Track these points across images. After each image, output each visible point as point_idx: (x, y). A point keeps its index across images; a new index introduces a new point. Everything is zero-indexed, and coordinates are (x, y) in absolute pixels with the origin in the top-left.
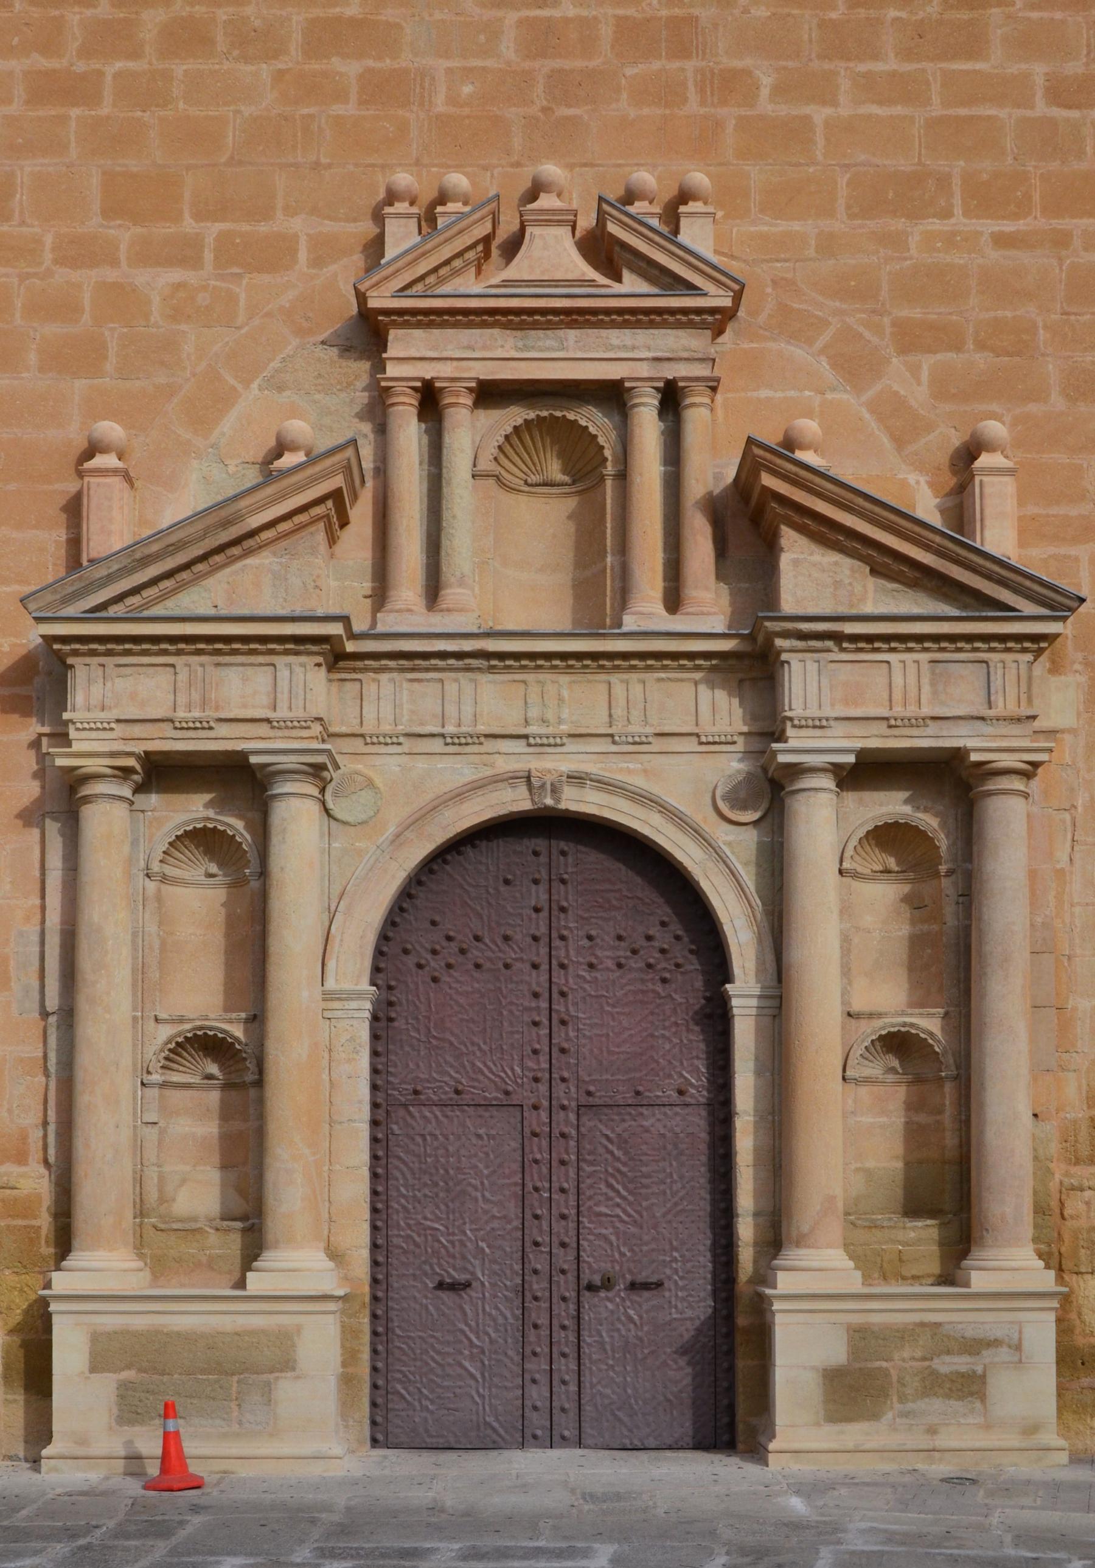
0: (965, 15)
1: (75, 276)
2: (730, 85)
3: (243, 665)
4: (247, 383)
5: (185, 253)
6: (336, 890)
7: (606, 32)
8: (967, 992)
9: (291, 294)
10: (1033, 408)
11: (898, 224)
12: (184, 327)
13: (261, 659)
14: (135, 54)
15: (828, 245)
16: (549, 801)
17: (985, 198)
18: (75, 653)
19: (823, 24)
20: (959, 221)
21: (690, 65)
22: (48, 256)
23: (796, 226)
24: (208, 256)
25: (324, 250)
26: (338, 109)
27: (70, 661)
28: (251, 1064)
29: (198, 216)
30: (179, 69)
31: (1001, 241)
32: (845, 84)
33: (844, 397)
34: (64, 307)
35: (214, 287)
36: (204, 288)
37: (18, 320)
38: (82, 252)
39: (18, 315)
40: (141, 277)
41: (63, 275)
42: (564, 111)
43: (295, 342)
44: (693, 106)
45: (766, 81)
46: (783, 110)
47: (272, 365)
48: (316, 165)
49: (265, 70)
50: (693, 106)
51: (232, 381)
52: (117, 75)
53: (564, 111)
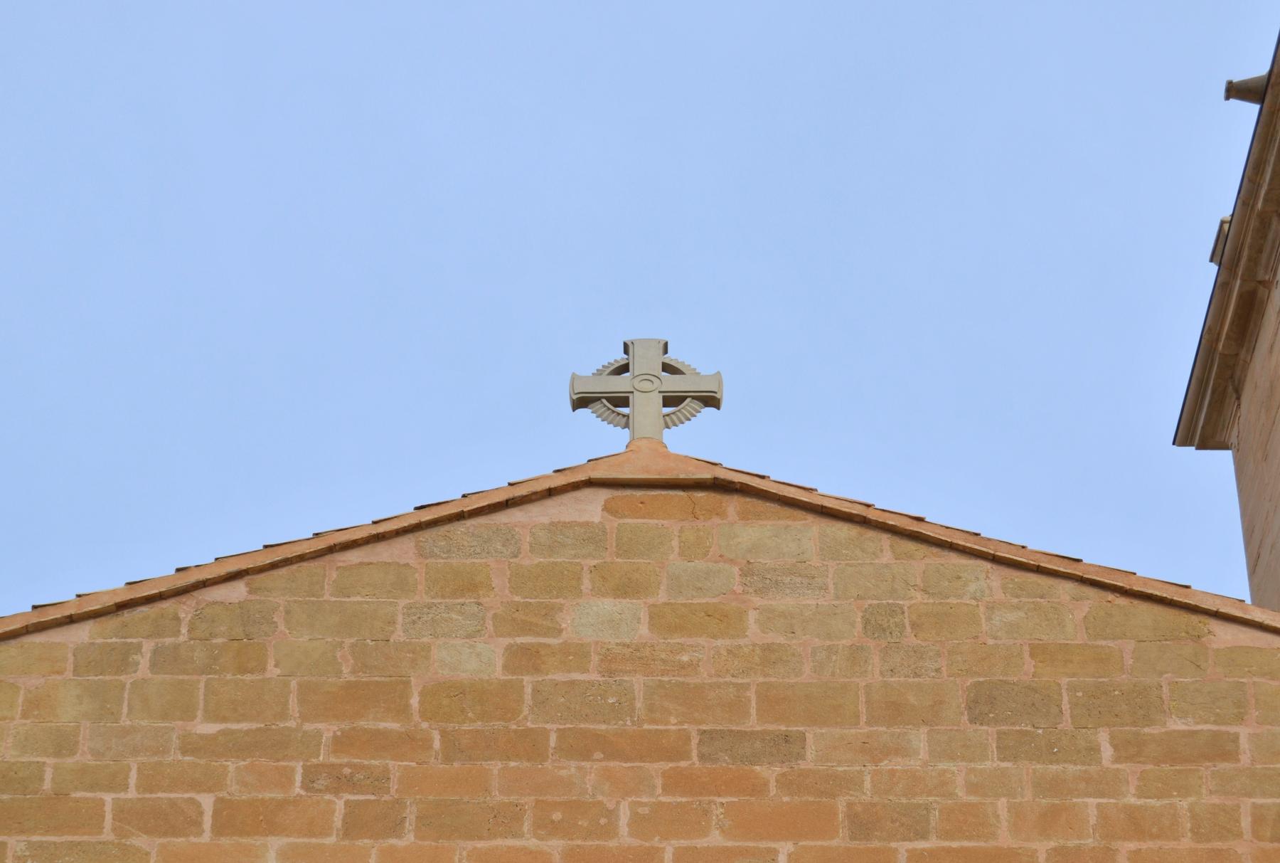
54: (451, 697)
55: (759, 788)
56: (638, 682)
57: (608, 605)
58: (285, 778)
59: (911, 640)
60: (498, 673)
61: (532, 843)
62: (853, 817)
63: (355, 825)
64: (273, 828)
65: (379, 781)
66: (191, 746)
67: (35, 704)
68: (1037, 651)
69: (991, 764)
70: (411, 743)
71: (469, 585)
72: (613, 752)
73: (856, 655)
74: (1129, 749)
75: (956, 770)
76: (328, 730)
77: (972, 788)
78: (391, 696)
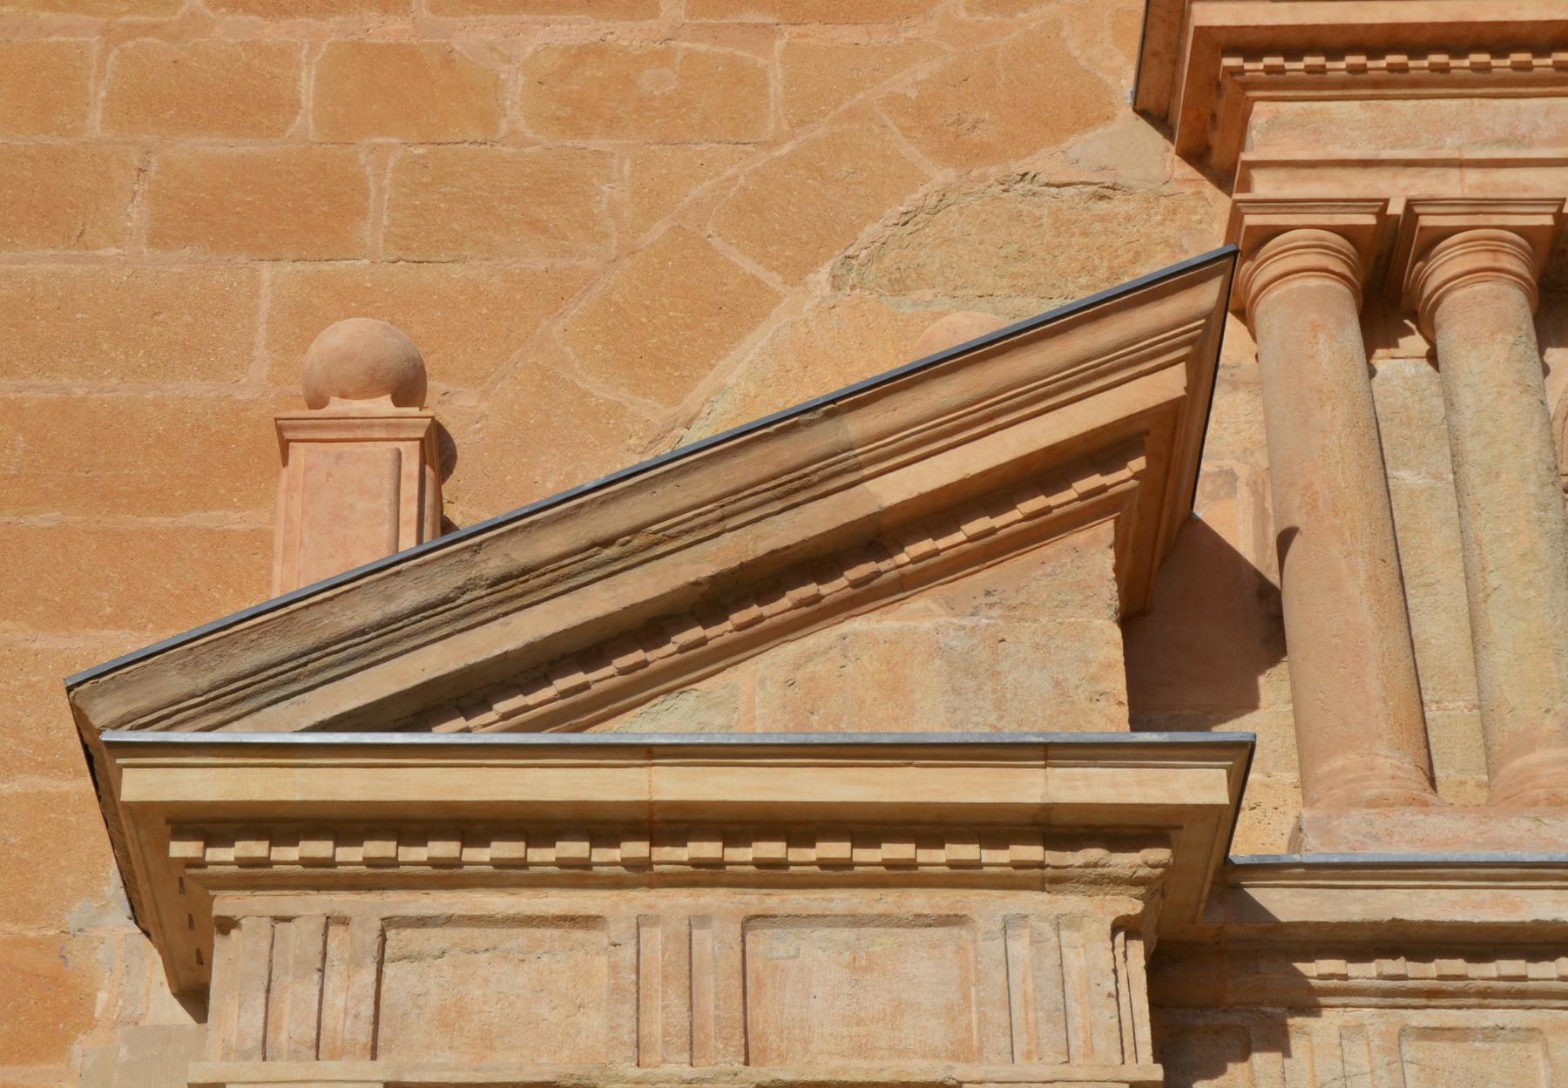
3: (855, 920)
4: (797, 272)
9: (924, 70)
12: (598, 143)
13: (919, 901)
18: (254, 877)
27: (226, 903)
35: (690, 56)
36: (663, 58)
39: (96, 116)
43: (942, 175)
47: (872, 229)
51: (749, 266)
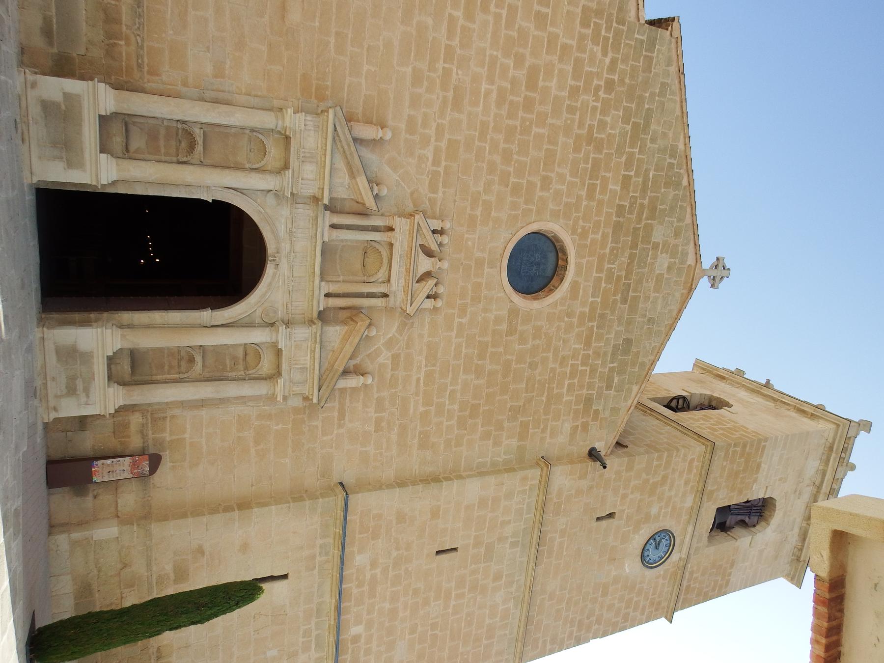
0: (473, 369)
1: (434, 128)
2: (463, 311)
5: (436, 162)
6: (244, 192)
7: (479, 280)
8: (208, 380)
10: (375, 389)
11: (425, 353)
14: (490, 153)
15: (421, 336)
16: (270, 258)
17: (429, 375)
19: (475, 335)
20: (424, 369)
21: (469, 301)
22: (440, 121)
23: (426, 328)
24: (435, 168)
25: (432, 202)
26: (469, 209)
28: (185, 159)
29: (446, 167)
30: (485, 165)
31: (418, 380)
32: (460, 340)
33: (382, 341)
34: (425, 125)
37: (423, 110)
38: (440, 131)
40: (431, 148)
41: (434, 126)
42: (461, 268)
44: (459, 302)
45: (464, 320)
46: (455, 325)
48: (455, 201)
49: (481, 189)
50: (459, 302)
52: (485, 147)
53: (461, 268)
54: (649, 229)
55: (614, 295)
56: (646, 270)
57: (666, 265)
58: (634, 192)
59: (646, 327)
60: (653, 240)
61: (609, 245)
62: (604, 314)
63: (621, 208)
64: (622, 189)
65: (630, 212)
66: (647, 171)
67: (665, 135)
68: (638, 352)
69: (613, 342)
70: (639, 220)
71: (677, 234)
72: (629, 264)
73: (644, 316)
74: (612, 370)
75: (612, 336)
76: (646, 202)
77: (607, 339)
78: (652, 217)
